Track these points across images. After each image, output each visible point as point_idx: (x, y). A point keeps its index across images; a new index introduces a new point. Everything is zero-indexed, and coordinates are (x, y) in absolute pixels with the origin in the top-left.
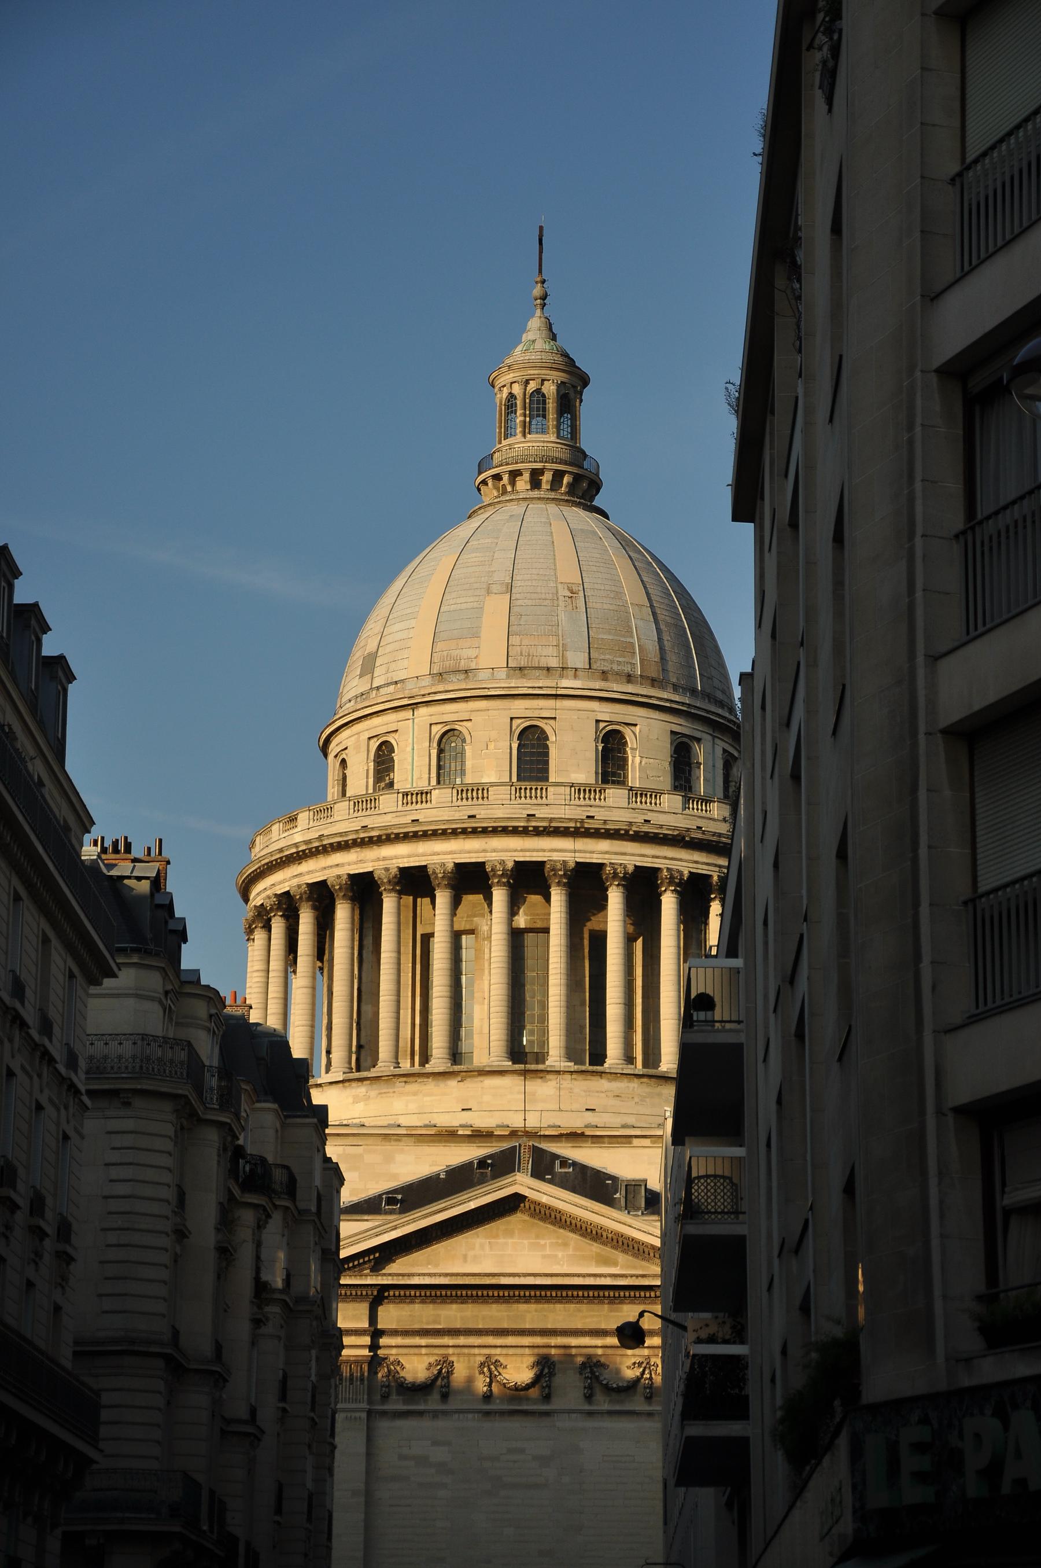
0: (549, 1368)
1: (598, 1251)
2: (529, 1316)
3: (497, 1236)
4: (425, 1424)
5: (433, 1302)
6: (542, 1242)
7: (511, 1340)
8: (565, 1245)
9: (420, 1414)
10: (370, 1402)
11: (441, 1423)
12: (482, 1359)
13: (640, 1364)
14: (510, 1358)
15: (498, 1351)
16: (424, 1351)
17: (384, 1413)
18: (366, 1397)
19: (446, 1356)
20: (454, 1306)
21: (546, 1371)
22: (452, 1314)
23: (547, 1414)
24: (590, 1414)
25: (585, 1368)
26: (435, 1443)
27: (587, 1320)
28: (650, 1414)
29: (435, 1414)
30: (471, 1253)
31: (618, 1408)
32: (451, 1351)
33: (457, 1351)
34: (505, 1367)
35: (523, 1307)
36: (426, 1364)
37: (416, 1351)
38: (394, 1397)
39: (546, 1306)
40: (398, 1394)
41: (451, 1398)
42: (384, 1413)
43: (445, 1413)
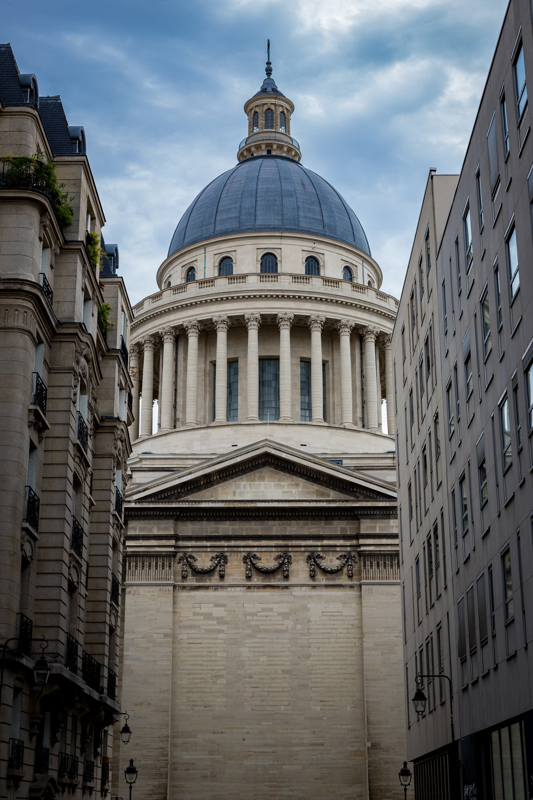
0: (288, 559)
1: (318, 488)
2: (274, 528)
3: (254, 480)
4: (211, 593)
5: (215, 520)
6: (282, 483)
7: (263, 543)
8: (297, 485)
9: (207, 588)
10: (175, 580)
11: (220, 593)
12: (245, 554)
13: (345, 556)
14: (263, 554)
15: (255, 549)
16: (209, 549)
17: (184, 587)
18: (172, 577)
19: (222, 553)
20: (228, 523)
21: (286, 561)
22: (226, 527)
23: (287, 587)
24: (314, 587)
25: (311, 559)
26: (217, 605)
27: (312, 530)
28: (352, 587)
29: (216, 588)
30: (238, 491)
31: (331, 583)
32: (226, 549)
33: (230, 549)
34: (260, 559)
35: (271, 523)
36: (210, 557)
37: (204, 549)
38: (190, 577)
39: (285, 522)
40: (193, 575)
41: (226, 577)
42: (184, 587)
43: (222, 587)
